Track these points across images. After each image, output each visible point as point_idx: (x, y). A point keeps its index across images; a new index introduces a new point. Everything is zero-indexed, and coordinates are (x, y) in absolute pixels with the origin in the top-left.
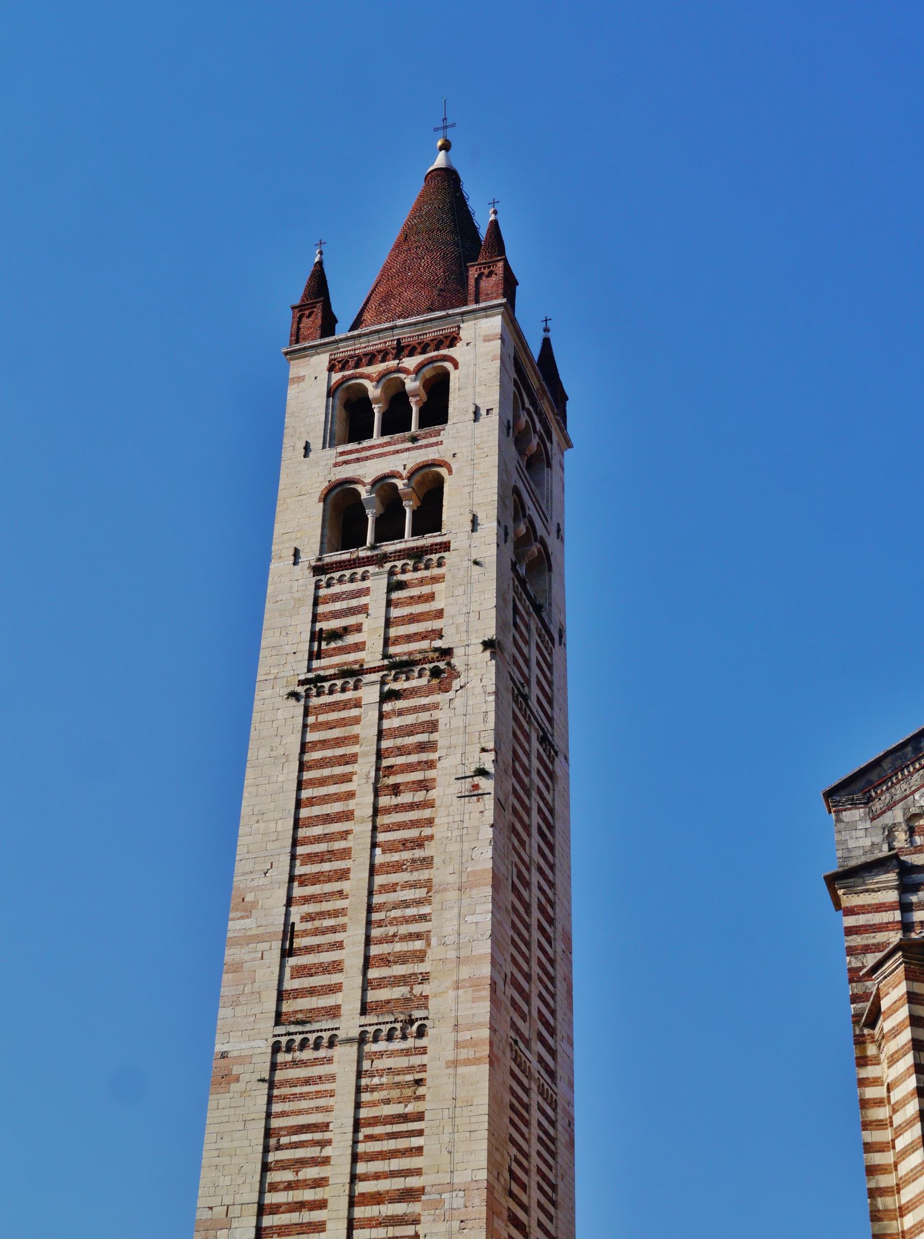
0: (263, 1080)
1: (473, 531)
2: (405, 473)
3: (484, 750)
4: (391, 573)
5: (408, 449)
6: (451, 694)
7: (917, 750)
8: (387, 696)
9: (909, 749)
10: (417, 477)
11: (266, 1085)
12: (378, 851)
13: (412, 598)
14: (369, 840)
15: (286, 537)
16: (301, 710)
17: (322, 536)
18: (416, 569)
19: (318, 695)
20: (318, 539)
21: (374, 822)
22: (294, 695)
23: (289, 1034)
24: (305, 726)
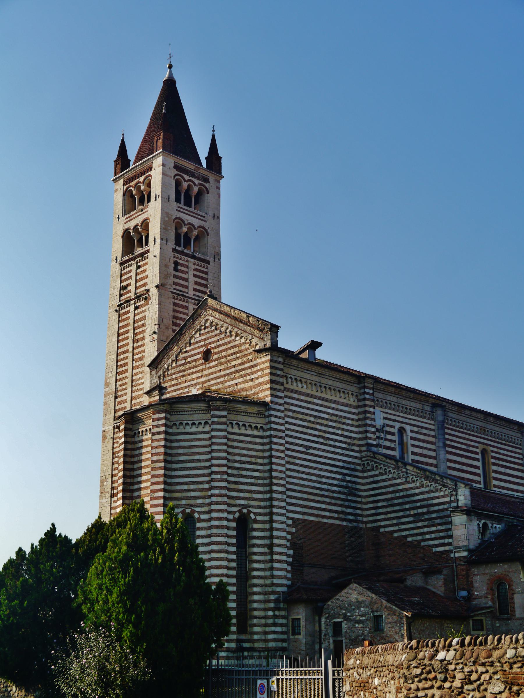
0: (111, 438)
1: (154, 244)
2: (140, 224)
3: (155, 325)
4: (137, 263)
5: (141, 214)
6: (149, 306)
7: (167, 350)
8: (136, 308)
9: (165, 350)
10: (144, 224)
11: (112, 439)
12: (134, 362)
13: (141, 271)
14: (132, 359)
15: (114, 253)
16: (118, 316)
17: (122, 251)
18: (142, 261)
19: (122, 310)
20: (121, 253)
21: (133, 352)
22: (116, 311)
23: (116, 423)
24: (119, 321)
